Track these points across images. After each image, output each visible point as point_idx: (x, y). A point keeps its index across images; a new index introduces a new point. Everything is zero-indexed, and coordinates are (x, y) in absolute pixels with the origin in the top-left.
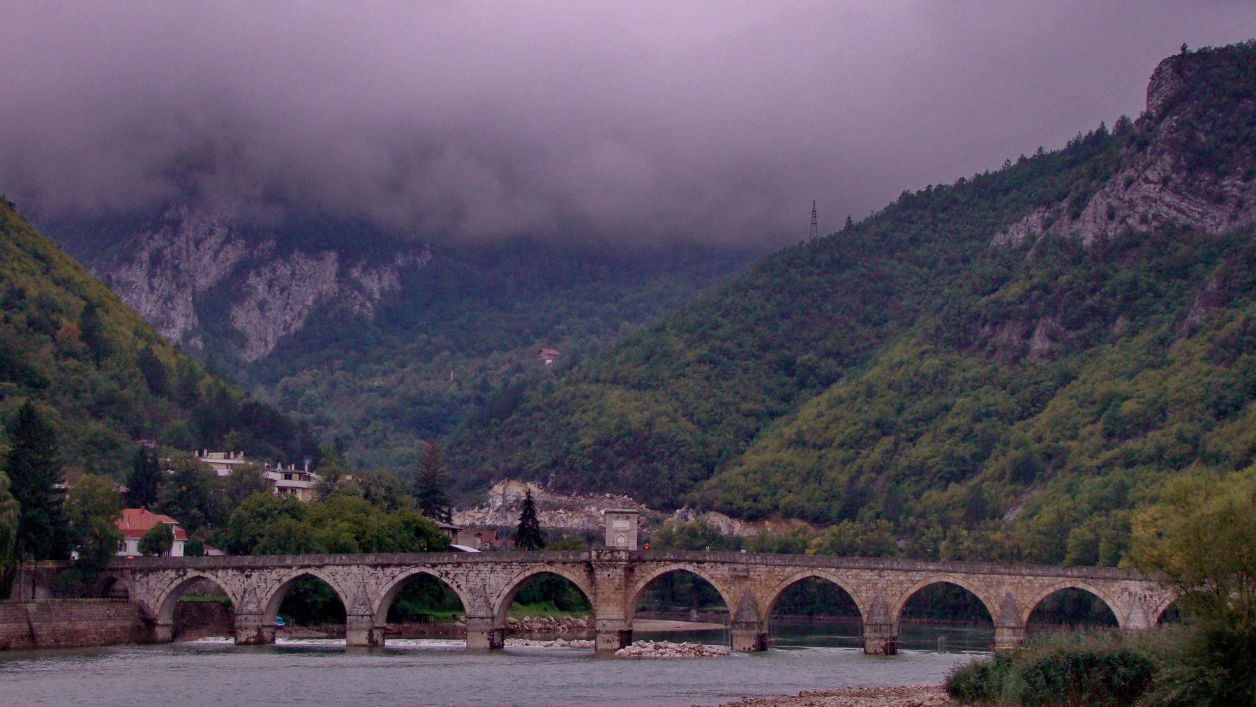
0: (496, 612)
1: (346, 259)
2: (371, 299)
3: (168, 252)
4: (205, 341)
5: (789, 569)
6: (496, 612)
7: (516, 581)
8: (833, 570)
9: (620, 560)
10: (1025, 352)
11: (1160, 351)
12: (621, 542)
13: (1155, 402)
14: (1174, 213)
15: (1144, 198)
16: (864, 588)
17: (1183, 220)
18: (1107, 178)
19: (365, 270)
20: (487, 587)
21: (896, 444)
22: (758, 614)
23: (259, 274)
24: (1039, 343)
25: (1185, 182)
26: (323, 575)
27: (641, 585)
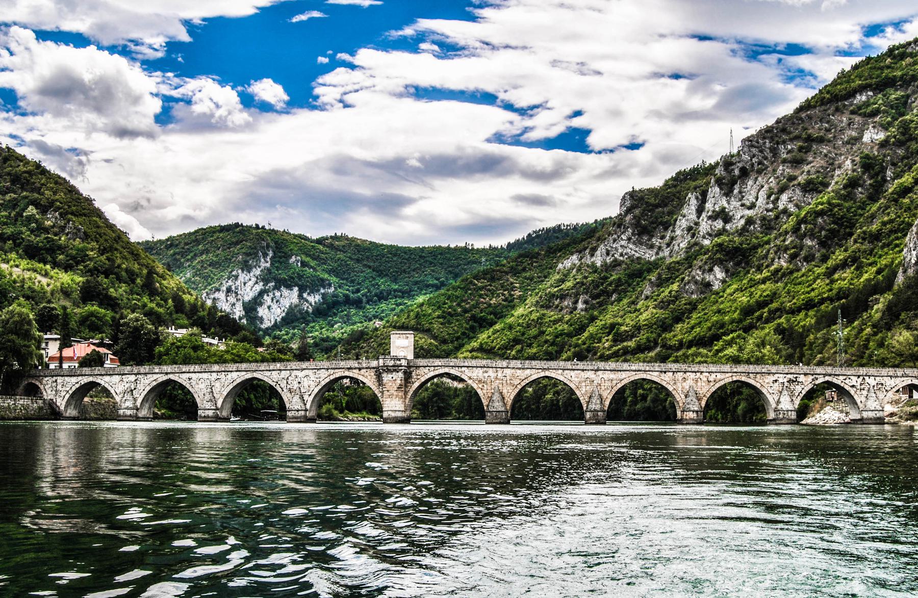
0: (308, 406)
1: (302, 290)
2: (311, 305)
3: (233, 288)
4: (247, 320)
5: (528, 372)
6: (308, 406)
7: (323, 383)
8: (560, 371)
9: (401, 366)
10: (575, 309)
11: (633, 306)
12: (401, 354)
13: (635, 326)
14: (633, 252)
15: (621, 246)
16: (584, 384)
17: (637, 255)
18: (605, 239)
19: (309, 294)
20: (302, 388)
21: (522, 348)
22: (505, 404)
23: (268, 295)
24: (580, 305)
25: (637, 239)
26: (182, 379)
27: (416, 385)
